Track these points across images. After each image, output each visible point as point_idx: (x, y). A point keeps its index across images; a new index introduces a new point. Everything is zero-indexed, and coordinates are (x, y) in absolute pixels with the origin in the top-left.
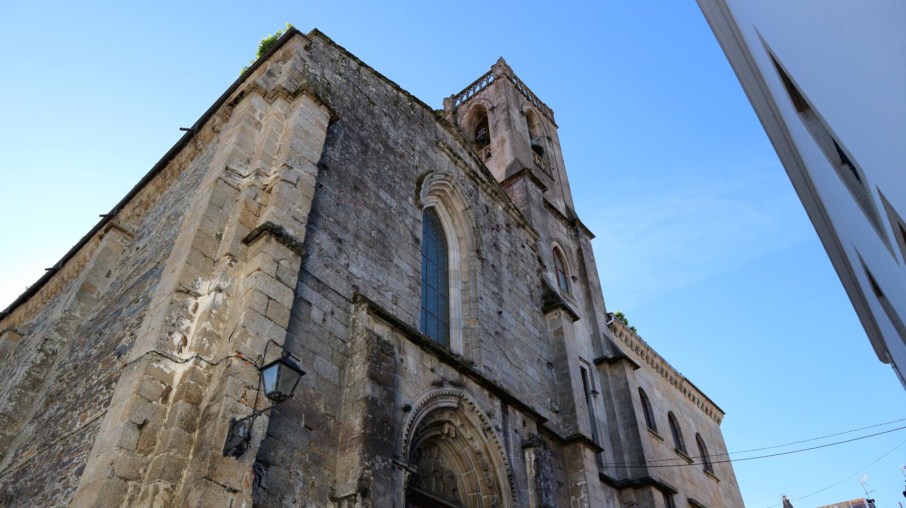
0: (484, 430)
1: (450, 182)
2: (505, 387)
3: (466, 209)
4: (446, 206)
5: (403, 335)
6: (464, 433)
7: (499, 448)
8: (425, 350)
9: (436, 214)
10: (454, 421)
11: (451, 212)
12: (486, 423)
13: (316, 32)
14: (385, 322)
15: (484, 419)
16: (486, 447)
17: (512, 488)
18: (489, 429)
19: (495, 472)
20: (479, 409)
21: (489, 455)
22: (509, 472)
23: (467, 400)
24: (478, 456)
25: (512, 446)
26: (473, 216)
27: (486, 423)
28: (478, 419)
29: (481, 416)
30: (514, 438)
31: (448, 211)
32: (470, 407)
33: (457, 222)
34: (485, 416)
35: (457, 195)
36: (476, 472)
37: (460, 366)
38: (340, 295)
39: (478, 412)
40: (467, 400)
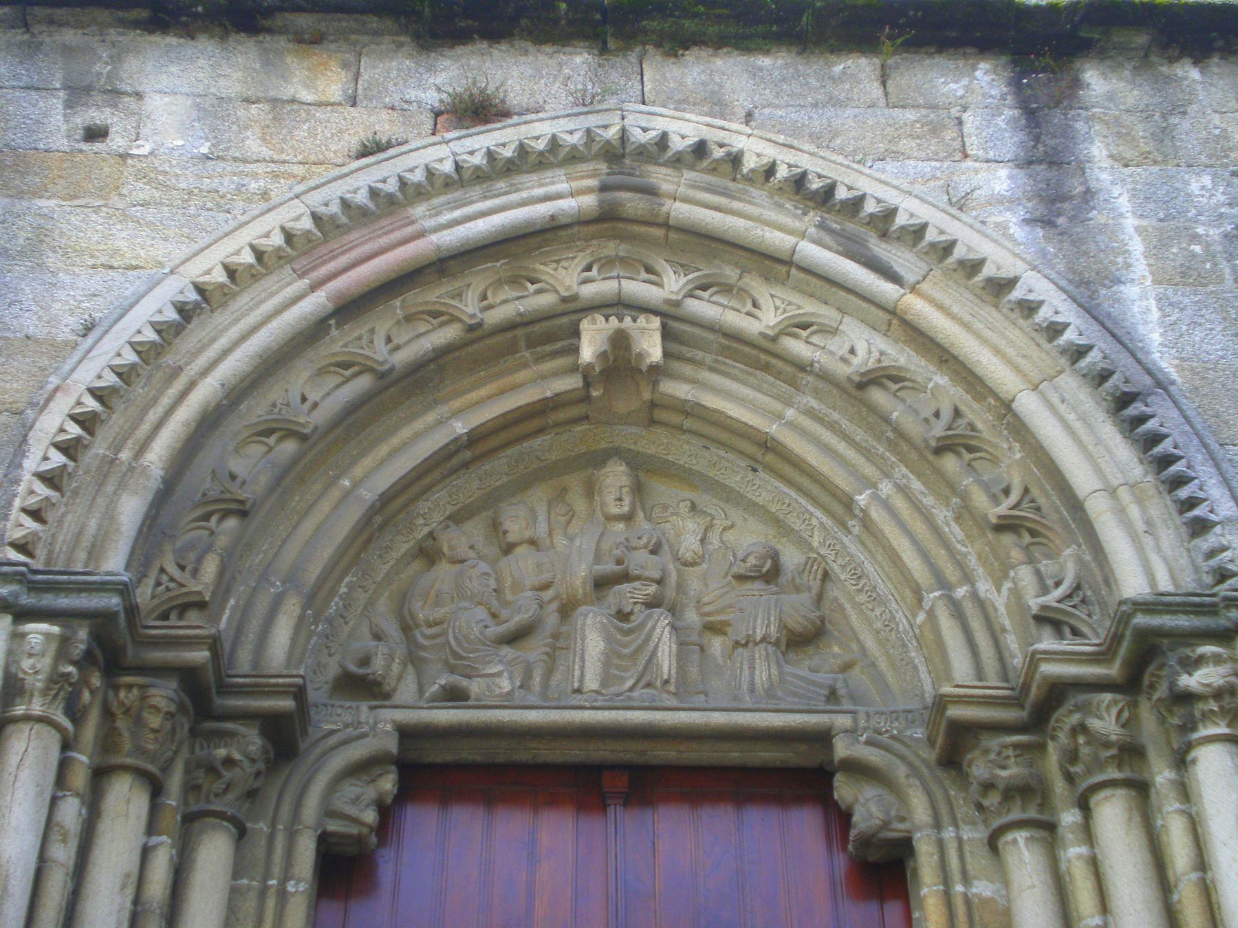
15: (830, 190)
19: (1019, 429)
20: (771, 152)
21: (944, 356)
25: (1137, 246)
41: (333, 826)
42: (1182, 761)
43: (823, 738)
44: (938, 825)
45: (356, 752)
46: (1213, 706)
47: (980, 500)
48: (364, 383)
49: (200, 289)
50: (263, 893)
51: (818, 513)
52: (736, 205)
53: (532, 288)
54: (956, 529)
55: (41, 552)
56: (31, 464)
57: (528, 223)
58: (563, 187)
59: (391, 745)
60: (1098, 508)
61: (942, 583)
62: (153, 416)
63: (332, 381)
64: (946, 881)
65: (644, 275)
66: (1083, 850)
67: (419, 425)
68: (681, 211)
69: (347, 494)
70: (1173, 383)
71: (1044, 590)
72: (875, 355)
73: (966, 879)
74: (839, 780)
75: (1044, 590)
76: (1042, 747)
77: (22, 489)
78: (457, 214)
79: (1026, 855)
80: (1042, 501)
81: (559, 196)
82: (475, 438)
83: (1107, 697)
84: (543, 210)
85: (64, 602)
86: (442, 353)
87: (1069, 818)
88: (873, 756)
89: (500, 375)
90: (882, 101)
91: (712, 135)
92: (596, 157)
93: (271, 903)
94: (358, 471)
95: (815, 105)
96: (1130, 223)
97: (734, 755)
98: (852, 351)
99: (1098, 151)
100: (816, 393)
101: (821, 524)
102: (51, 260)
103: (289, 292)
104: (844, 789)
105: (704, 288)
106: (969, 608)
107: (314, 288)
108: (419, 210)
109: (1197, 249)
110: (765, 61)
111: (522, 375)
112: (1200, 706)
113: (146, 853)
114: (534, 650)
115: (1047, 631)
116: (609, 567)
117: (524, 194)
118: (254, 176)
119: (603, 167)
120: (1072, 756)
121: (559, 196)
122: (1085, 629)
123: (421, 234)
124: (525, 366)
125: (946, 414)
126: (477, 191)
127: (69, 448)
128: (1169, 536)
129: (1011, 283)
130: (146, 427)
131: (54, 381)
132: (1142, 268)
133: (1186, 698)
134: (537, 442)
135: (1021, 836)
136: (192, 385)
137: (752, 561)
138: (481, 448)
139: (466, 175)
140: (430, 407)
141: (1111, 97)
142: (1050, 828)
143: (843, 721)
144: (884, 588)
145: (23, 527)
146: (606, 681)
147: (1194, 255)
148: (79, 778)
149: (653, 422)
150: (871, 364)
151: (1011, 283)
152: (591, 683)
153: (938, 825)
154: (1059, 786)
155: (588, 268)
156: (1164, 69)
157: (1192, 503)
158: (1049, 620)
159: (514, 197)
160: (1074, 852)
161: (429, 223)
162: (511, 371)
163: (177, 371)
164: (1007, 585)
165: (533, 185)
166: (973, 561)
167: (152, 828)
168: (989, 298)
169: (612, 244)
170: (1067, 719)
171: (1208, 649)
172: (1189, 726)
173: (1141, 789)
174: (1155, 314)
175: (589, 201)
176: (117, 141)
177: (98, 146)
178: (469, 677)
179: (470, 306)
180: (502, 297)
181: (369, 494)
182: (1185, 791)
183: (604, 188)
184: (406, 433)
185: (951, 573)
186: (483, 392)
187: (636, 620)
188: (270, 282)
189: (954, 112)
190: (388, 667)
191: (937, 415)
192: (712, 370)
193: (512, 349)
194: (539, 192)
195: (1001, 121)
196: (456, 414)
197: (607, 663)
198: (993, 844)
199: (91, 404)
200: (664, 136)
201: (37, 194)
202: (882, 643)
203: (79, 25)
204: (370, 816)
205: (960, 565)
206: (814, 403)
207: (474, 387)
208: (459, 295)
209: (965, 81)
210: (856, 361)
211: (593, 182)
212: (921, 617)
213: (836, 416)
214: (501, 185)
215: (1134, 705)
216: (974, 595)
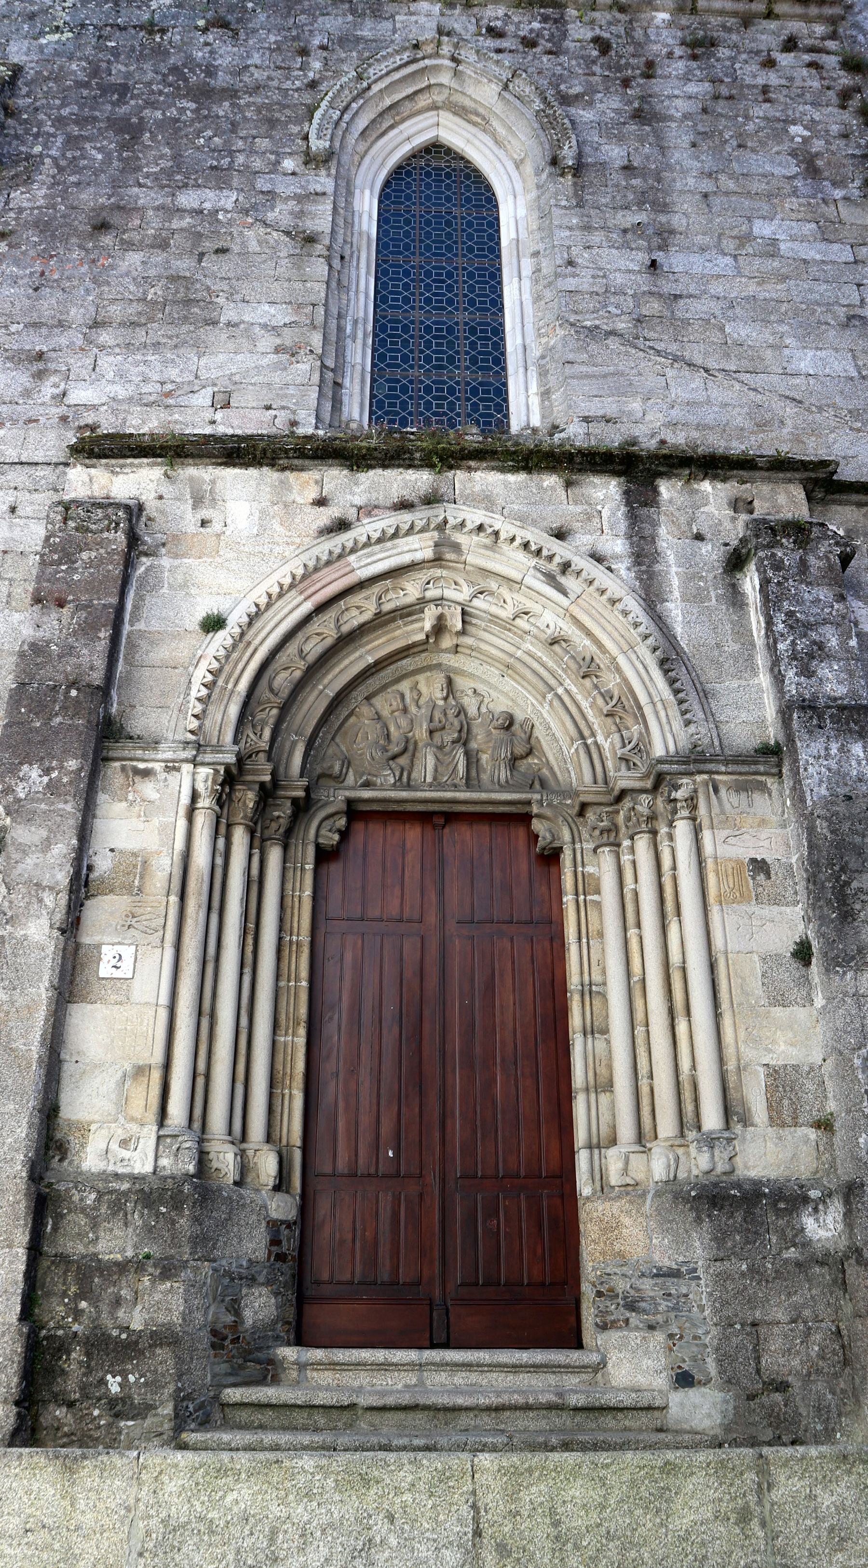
0: (550, 579)
1: (437, 55)
2: (678, 439)
3: (506, 87)
4: (461, 112)
5: (207, 465)
6: (494, 610)
7: (613, 602)
8: (283, 469)
9: (449, 151)
10: (449, 593)
11: (479, 121)
12: (550, 558)
14: (137, 461)
16: (573, 617)
17: (676, 692)
18: (566, 567)
22: (658, 653)
23: (463, 524)
24: (556, 647)
25: (675, 582)
26: (527, 90)
27: (550, 558)
28: (521, 556)
29: (526, 546)
30: (686, 560)
31: (475, 124)
32: (483, 539)
33: (501, 131)
34: (537, 537)
35: (469, 72)
36: (574, 689)
37: (418, 455)
38: (37, 464)
39: (513, 539)
40: (463, 524)
42: (671, 824)
43: (529, 803)
44: (573, 842)
45: (330, 810)
46: (684, 804)
47: (600, 701)
50: (295, 869)
51: (531, 698)
52: (497, 556)
53: (402, 593)
54: (590, 711)
56: (194, 694)
58: (417, 546)
59: (344, 807)
60: (648, 710)
61: (582, 737)
62: (240, 666)
64: (575, 866)
65: (454, 586)
66: (630, 857)
69: (321, 692)
70: (685, 653)
71: (624, 746)
72: (558, 629)
73: (583, 865)
74: (534, 821)
75: (624, 746)
76: (618, 812)
77: (191, 706)
78: (369, 560)
79: (608, 858)
80: (626, 703)
81: (416, 550)
83: (644, 796)
84: (406, 559)
87: (626, 843)
88: (548, 812)
89: (388, 632)
90: (565, 502)
91: (487, 521)
92: (433, 530)
93: (299, 873)
94: (326, 681)
95: (535, 503)
96: (674, 569)
97: (490, 809)
98: (548, 626)
99: (663, 531)
100: (532, 643)
101: (533, 704)
102: (193, 591)
103: (295, 602)
104: (537, 825)
105: (481, 593)
106: (593, 749)
107: (305, 599)
108: (352, 558)
109: (702, 584)
111: (398, 633)
112: (679, 805)
113: (250, 856)
114: (403, 761)
115: (623, 766)
116: (436, 724)
117: (399, 550)
119: (436, 534)
120: (628, 819)
121: (416, 550)
122: (639, 764)
123: (353, 571)
124: (399, 627)
125: (588, 659)
126: (377, 548)
127: (209, 686)
128: (677, 723)
129: (620, 600)
130: (238, 672)
131: (200, 652)
132: (677, 594)
133: (675, 800)
134: (404, 662)
135: (607, 849)
136: (255, 650)
137: (500, 721)
138: (379, 667)
139: (373, 541)
140: (356, 649)
141: (670, 501)
142: (619, 845)
143: (537, 796)
144: (558, 734)
145: (194, 724)
146: (435, 779)
147: (700, 587)
148: (223, 829)
149: (457, 652)
150: (556, 634)
151: (620, 600)
152: (429, 779)
153: (573, 842)
154: (623, 830)
155: (428, 583)
156: (696, 486)
157: (686, 712)
158: (624, 759)
159: (395, 551)
160: (626, 858)
161: (355, 565)
162: (394, 630)
163: (249, 643)
164: (609, 740)
165: (403, 543)
166: (596, 727)
167: (251, 847)
168: (609, 607)
169: (439, 571)
170: (627, 803)
171: (685, 781)
172: (675, 811)
173: (654, 833)
174: (680, 619)
175: (428, 554)
176: (216, 527)
177: (208, 530)
178: (376, 776)
180: (388, 598)
181: (331, 693)
182: (671, 837)
183: (437, 545)
184: (346, 662)
185: (586, 733)
186: (380, 641)
187: (447, 749)
189: (599, 508)
191: (584, 659)
192: (485, 630)
193: (394, 620)
194: (406, 549)
195: (619, 514)
196: (369, 652)
197: (436, 770)
198: (595, 851)
200: (464, 521)
201: (183, 556)
202: (556, 759)
203: (195, 465)
204: (336, 837)
205: (590, 728)
206: (531, 648)
207: (376, 639)
209: (604, 491)
210: (549, 632)
211: (431, 543)
212: (573, 750)
213: (539, 654)
214: (389, 544)
215: (655, 798)
216: (596, 743)
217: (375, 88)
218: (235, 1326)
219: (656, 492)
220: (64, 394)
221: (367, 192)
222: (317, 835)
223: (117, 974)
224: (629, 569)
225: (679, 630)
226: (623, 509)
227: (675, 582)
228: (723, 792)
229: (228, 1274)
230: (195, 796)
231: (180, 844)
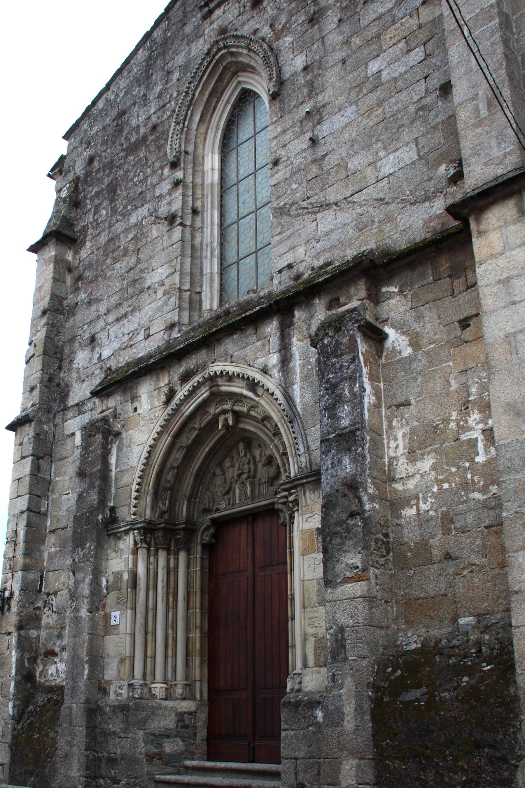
13: (67, 137)
15: (243, 376)
25: (298, 371)
41: (204, 542)
48: (185, 450)
49: (150, 446)
52: (232, 384)
55: (138, 513)
56: (133, 497)
57: (183, 421)
59: (210, 524)
63: (180, 451)
67: (201, 451)
68: (223, 388)
82: (211, 450)
85: (137, 526)
86: (197, 436)
96: (298, 363)
99: (294, 340)
107: (169, 435)
110: (235, 337)
118: (156, 412)
119: (209, 382)
148: (152, 553)
171: (293, 491)
179: (197, 426)
183: (211, 388)
184: (199, 454)
188: (162, 437)
190: (209, 505)
196: (207, 446)
199: (139, 480)
208: (195, 423)
211: (208, 388)
214: (194, 395)
217: (197, 94)
218: (159, 754)
219: (293, 316)
220: (101, 355)
221: (210, 155)
222: (202, 539)
223: (116, 623)
224: (279, 371)
225: (298, 400)
226: (278, 334)
227: (298, 371)
228: (307, 493)
229: (153, 734)
230: (136, 543)
231: (130, 566)
